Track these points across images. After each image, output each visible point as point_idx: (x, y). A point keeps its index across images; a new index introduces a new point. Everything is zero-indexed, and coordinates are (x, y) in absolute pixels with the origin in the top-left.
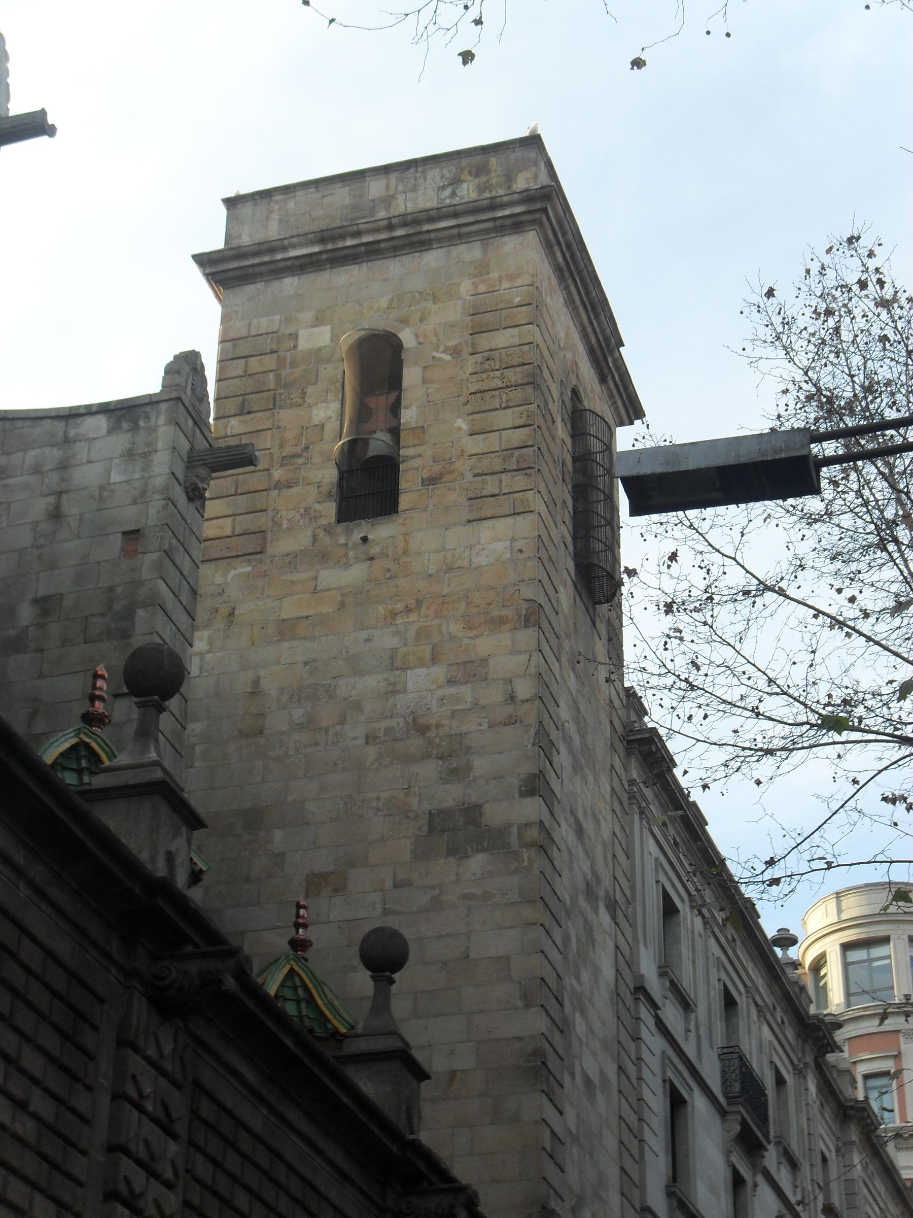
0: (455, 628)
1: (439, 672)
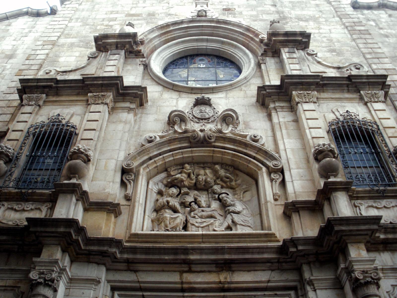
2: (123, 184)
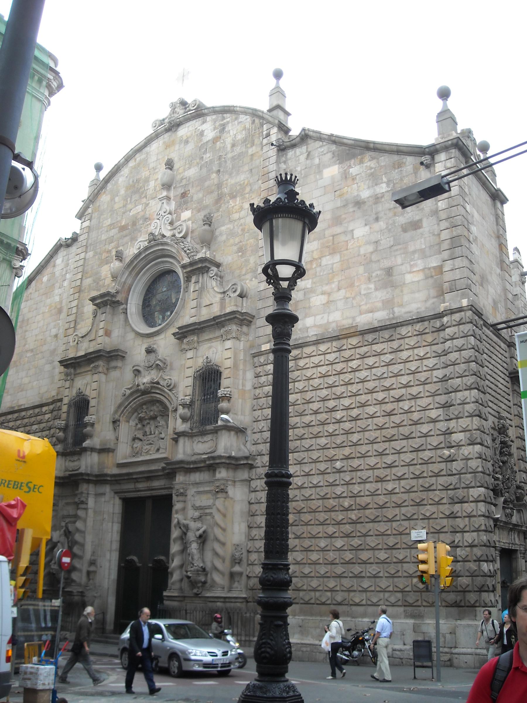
2: (115, 429)
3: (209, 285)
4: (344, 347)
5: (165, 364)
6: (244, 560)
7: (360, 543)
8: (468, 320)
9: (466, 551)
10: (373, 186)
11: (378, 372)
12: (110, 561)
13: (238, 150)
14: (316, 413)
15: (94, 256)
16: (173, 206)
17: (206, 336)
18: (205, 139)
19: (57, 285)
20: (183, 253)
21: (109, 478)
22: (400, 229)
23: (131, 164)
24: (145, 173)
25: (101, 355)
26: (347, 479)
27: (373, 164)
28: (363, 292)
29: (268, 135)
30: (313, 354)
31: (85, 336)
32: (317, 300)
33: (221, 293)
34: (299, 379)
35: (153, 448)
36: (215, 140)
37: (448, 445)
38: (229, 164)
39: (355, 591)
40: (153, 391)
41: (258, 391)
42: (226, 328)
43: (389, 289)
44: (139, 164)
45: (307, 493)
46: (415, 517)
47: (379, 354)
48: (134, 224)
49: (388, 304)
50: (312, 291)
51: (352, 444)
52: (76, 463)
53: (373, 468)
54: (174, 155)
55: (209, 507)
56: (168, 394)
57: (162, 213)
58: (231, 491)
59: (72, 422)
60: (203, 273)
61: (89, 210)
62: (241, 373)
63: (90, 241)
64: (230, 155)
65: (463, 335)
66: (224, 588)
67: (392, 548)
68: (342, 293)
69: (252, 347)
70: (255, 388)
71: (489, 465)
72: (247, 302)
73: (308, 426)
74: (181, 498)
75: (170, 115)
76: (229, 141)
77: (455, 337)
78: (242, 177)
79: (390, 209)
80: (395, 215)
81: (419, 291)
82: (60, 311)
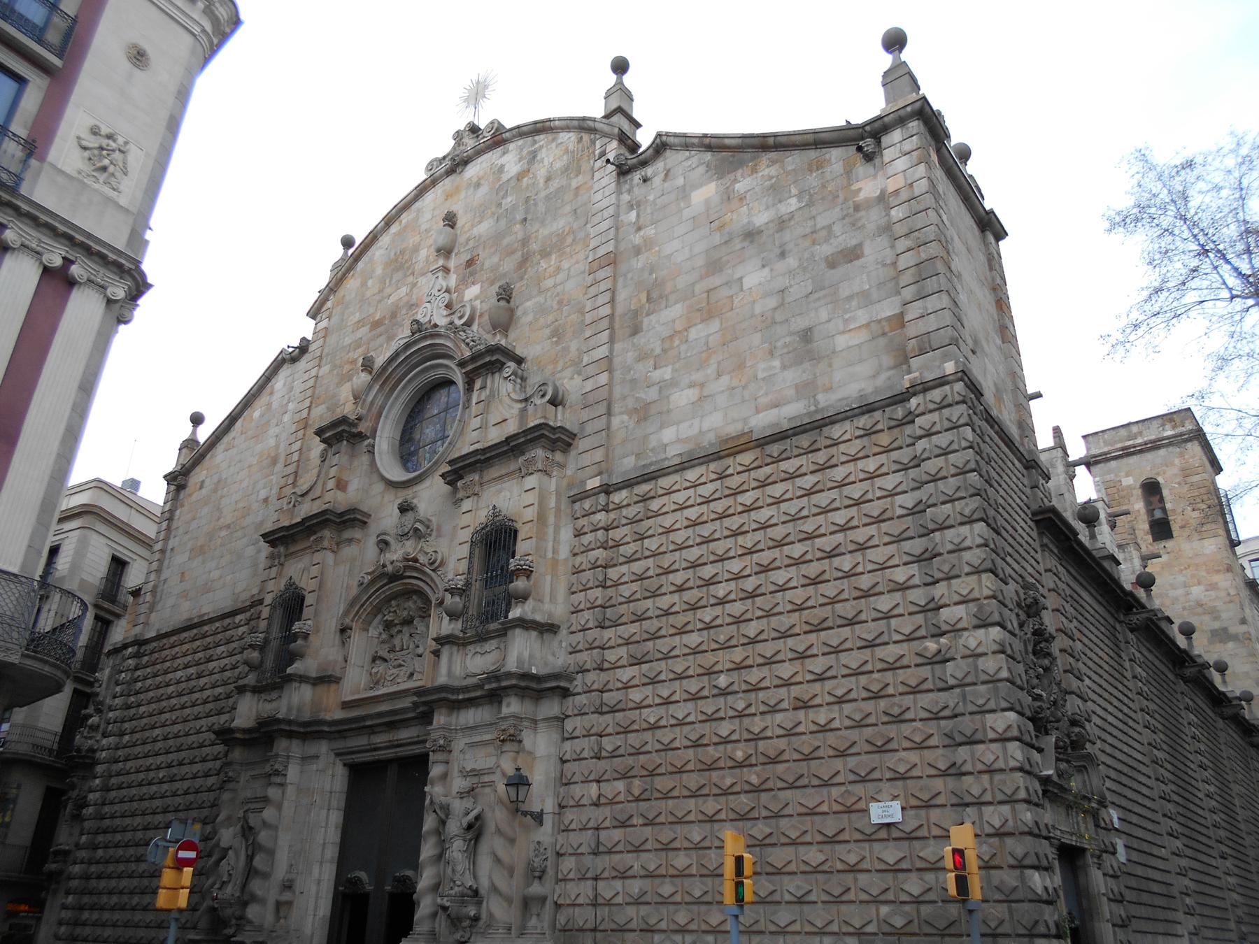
0: (1204, 574)
1: (1202, 588)
3: (503, 392)
4: (730, 471)
5: (428, 527)
6: (550, 872)
7: (768, 831)
8: (958, 398)
9: (991, 846)
10: (774, 205)
11: (792, 507)
12: (319, 882)
13: (555, 184)
14: (680, 589)
15: (331, 371)
16: (453, 280)
17: (494, 472)
18: (505, 177)
19: (274, 421)
20: (463, 346)
21: (326, 729)
22: (823, 265)
23: (394, 228)
24: (412, 240)
25: (327, 520)
26: (740, 705)
27: (773, 171)
28: (761, 375)
29: (603, 154)
30: (675, 488)
31: (307, 493)
32: (682, 398)
33: (521, 401)
34: (650, 533)
35: (404, 672)
36: (520, 177)
37: (936, 631)
38: (541, 208)
39: (762, 932)
40: (407, 574)
41: (579, 559)
42: (527, 456)
43: (807, 365)
44: (405, 227)
45: (666, 736)
46: (876, 775)
47: (792, 477)
48: (394, 315)
49: (806, 389)
50: (673, 383)
51: (746, 641)
52: (274, 704)
53: (787, 684)
54: (457, 207)
55: (490, 771)
56: (432, 579)
57: (435, 292)
58: (528, 738)
59: (276, 633)
60: (493, 373)
61: (329, 304)
62: (551, 530)
63: (326, 350)
64: (542, 194)
65: (951, 425)
66: (510, 929)
67: (831, 841)
68: (725, 380)
69: (570, 486)
70: (575, 555)
71: (1021, 668)
72: (563, 414)
73: (667, 613)
74: (440, 756)
75: (454, 148)
76: (541, 173)
77: (934, 430)
78: (560, 224)
79: (805, 236)
80: (814, 243)
81: (861, 361)
82: (274, 461)
